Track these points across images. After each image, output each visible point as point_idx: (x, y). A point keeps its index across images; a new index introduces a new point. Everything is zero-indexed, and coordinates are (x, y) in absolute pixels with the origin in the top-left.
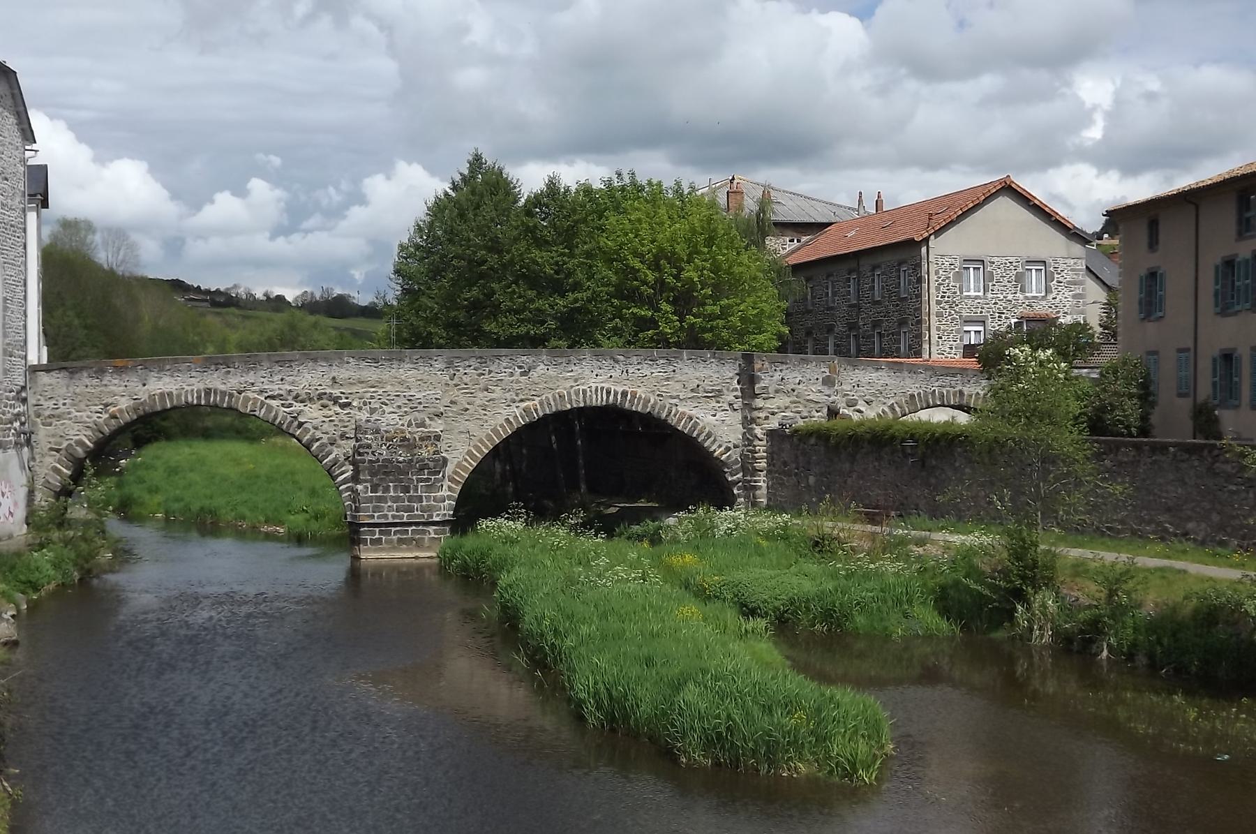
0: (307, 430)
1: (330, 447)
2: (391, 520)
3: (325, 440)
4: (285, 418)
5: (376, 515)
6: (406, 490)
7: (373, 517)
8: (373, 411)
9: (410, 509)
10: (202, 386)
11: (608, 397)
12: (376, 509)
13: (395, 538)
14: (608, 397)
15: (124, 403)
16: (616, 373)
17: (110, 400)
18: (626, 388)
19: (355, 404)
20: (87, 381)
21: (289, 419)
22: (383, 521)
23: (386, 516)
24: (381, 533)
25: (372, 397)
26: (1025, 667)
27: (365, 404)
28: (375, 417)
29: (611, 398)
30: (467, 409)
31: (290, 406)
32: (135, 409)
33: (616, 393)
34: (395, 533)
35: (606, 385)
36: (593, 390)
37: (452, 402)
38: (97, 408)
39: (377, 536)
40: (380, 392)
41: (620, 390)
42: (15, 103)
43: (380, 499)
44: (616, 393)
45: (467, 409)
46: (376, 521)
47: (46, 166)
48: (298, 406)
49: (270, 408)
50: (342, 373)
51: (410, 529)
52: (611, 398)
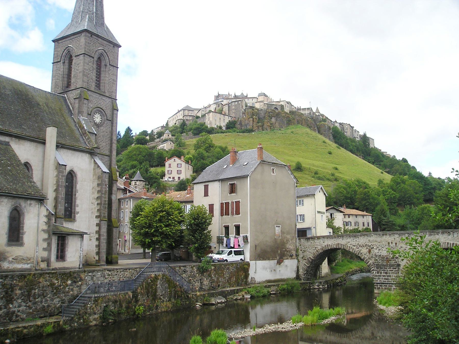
0: (363, 255)
1: (369, 260)
2: (382, 282)
3: (367, 258)
4: (357, 252)
5: (378, 280)
6: (386, 273)
7: (377, 281)
8: (379, 250)
9: (388, 279)
10: (337, 243)
11: (448, 245)
12: (379, 279)
13: (384, 287)
14: (448, 245)
15: (319, 247)
16: (450, 237)
17: (316, 247)
18: (454, 242)
19: (375, 248)
20: (311, 241)
21: (358, 252)
22: (380, 282)
23: (381, 281)
24: (380, 286)
25: (379, 246)
26: (213, 301)
27: (377, 248)
28: (380, 251)
29: (449, 245)
30: (405, 249)
31: (358, 248)
32: (322, 249)
33: (450, 244)
34: (384, 286)
35: (447, 241)
36: (443, 243)
37: (401, 247)
38: (314, 249)
39: (379, 287)
40: (381, 244)
41: (452, 243)
42: (119, 214)
43: (379, 276)
44: (450, 244)
45: (405, 249)
46: (378, 282)
47: (209, 205)
48: (360, 248)
49: (353, 249)
50: (371, 239)
51: (388, 285)
52: (449, 245)
